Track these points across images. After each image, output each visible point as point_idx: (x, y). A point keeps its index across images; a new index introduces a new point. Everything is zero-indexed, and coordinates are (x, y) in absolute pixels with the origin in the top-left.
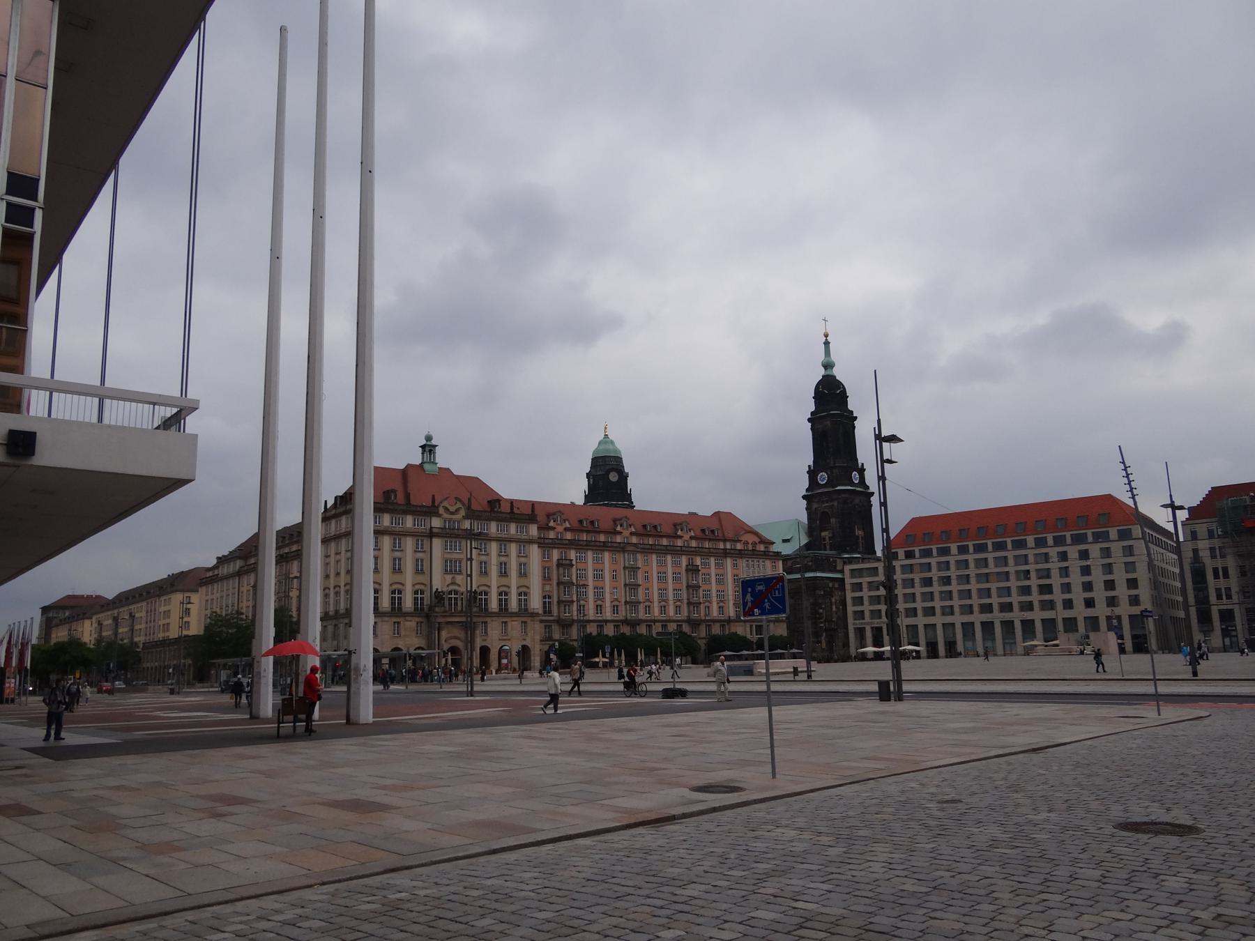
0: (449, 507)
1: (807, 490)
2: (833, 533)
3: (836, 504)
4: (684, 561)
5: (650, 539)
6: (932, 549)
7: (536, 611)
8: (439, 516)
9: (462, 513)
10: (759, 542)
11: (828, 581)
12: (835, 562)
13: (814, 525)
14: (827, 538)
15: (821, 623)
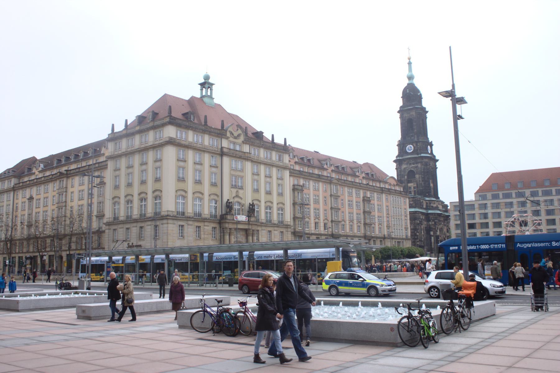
0: (233, 132)
1: (397, 157)
2: (417, 184)
3: (419, 165)
4: (361, 193)
5: (342, 176)
6: (512, 193)
7: (289, 223)
8: (227, 138)
9: (242, 138)
10: (396, 185)
11: (420, 215)
12: (422, 202)
13: (403, 179)
14: (412, 188)
15: (418, 242)
